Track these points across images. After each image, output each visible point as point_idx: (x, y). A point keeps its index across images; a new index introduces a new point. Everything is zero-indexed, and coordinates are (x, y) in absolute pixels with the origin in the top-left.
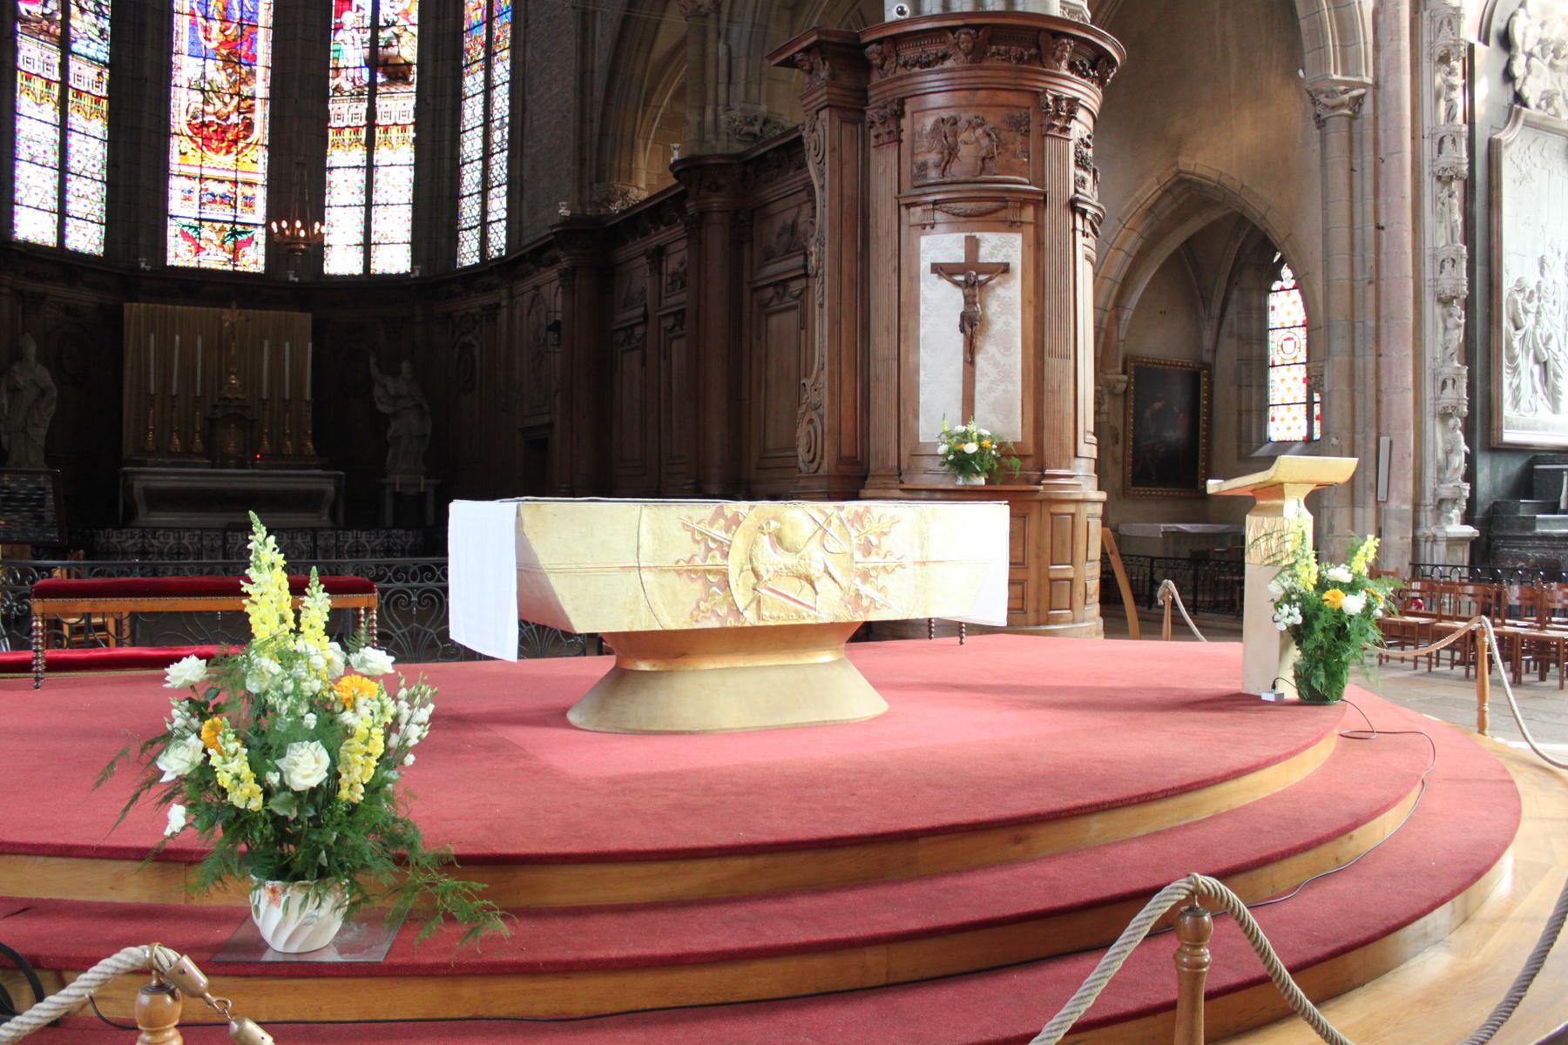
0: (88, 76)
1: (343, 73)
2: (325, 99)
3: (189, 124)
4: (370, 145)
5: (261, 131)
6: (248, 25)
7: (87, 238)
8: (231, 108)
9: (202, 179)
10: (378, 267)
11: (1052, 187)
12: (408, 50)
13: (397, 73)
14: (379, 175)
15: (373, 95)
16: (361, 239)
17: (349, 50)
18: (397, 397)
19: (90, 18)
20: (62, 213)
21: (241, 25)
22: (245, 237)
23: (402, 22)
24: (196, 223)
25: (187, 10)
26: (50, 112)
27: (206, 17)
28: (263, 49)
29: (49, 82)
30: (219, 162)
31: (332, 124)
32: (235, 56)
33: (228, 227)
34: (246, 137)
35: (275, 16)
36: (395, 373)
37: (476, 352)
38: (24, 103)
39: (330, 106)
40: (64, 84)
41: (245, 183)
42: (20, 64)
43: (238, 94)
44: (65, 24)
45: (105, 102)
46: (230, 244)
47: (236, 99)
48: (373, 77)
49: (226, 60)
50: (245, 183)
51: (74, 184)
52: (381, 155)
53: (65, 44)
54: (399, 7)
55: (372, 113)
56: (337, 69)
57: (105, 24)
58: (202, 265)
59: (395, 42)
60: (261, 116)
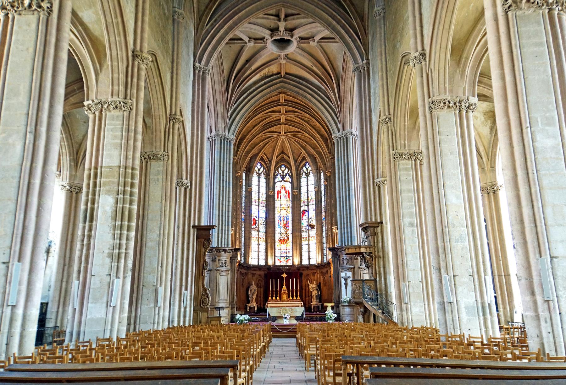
0: (262, 235)
2: (301, 232)
4: (309, 240)
5: (291, 240)
6: (288, 220)
7: (262, 263)
10: (311, 263)
12: (314, 223)
13: (312, 227)
17: (304, 223)
20: (258, 259)
26: (257, 242)
28: (290, 225)
30: (284, 246)
32: (286, 227)
36: (313, 283)
40: (258, 238)
44: (259, 228)
52: (311, 242)
53: (258, 231)
55: (309, 235)
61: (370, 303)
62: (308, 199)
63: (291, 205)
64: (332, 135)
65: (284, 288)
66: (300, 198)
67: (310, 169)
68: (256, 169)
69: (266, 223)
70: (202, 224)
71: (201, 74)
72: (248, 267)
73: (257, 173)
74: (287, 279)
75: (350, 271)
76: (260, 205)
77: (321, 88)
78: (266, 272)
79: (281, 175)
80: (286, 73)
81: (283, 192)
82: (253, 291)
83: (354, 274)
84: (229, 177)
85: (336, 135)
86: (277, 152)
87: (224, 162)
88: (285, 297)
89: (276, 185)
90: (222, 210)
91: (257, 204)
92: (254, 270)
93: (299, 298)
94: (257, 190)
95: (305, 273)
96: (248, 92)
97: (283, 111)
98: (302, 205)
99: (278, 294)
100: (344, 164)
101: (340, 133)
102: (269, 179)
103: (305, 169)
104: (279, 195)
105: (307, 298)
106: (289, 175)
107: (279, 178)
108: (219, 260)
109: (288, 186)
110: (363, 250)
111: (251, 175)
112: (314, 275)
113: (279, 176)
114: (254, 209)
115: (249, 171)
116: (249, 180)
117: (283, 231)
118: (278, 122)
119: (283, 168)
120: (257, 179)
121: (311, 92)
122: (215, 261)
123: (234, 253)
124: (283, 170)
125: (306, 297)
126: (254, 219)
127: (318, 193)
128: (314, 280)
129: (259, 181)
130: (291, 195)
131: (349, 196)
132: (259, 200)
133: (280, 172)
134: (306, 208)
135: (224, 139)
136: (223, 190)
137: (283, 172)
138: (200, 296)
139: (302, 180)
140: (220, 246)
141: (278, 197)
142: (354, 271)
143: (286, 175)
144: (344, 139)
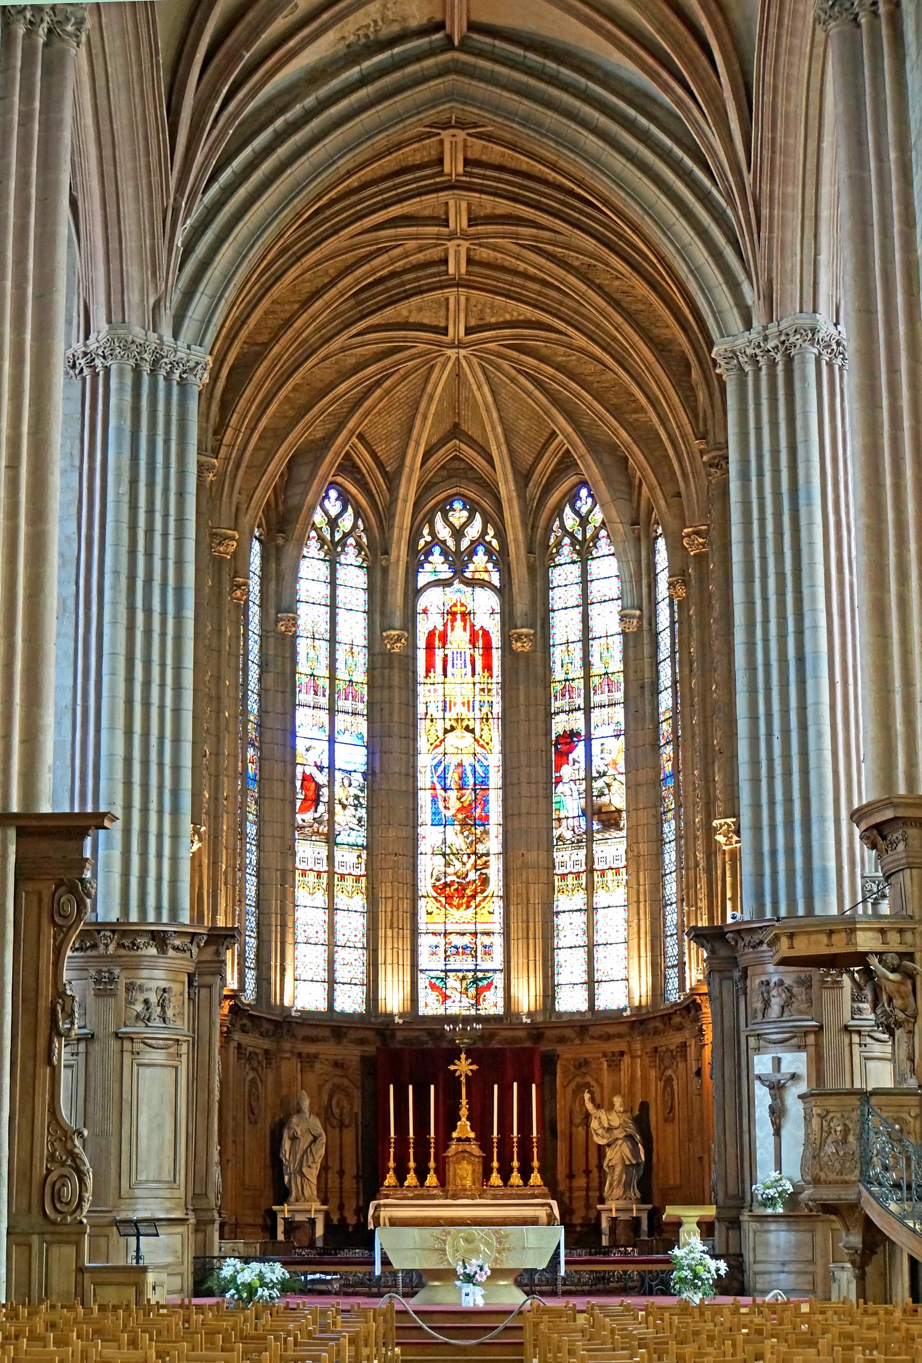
0: (349, 860)
1: (564, 822)
2: (550, 849)
3: (434, 886)
4: (590, 889)
5: (496, 885)
6: (482, 785)
7: (351, 1001)
8: (468, 866)
9: (446, 934)
10: (601, 1004)
11: (828, 1020)
13: (610, 820)
14: (600, 916)
15: (591, 840)
16: (585, 978)
17: (569, 801)
18: (610, 1129)
19: (351, 810)
20: (332, 982)
21: (475, 790)
22: (485, 982)
23: (611, 771)
24: (442, 975)
25: (429, 785)
26: (321, 899)
27: (445, 789)
29: (319, 874)
30: (460, 917)
31: (557, 871)
32: (471, 819)
33: (470, 975)
34: (483, 891)
35: (504, 777)
37: (675, 1083)
38: (302, 895)
39: (555, 854)
40: (331, 873)
41: (483, 933)
42: (297, 865)
43: (475, 853)
45: (363, 879)
46: (472, 991)
47: (473, 857)
48: (589, 824)
49: (463, 824)
50: (483, 933)
51: (341, 955)
53: (331, 840)
54: (609, 759)
56: (559, 820)
57: (362, 812)
58: (449, 1012)
59: (606, 791)
60: (495, 870)
61: (893, 1207)
62: (587, 677)
63: (497, 709)
64: (710, 344)
65: (464, 1129)
66: (548, 669)
67: (597, 517)
68: (319, 518)
69: (370, 798)
70: (46, 808)
71: (41, 41)
72: (277, 1024)
73: (321, 539)
74: (479, 1088)
75: (799, 1048)
76: (341, 704)
77: (654, 100)
78: (371, 1049)
79: (445, 553)
80: (473, 27)
81: (459, 637)
82: (304, 1143)
83: (817, 1062)
84: (180, 562)
85: (732, 340)
86: (424, 433)
87: (151, 484)
88: (465, 1172)
89: (423, 602)
90: (146, 734)
91: (324, 701)
92: (308, 1039)
93: (536, 1178)
94: (323, 628)
95: (566, 1054)
96: (279, 123)
97: (459, 221)
98: (555, 705)
99: (427, 1160)
100: (777, 494)
101: (754, 335)
102: (385, 571)
103: (570, 520)
104: (439, 654)
105: (581, 1182)
106: (489, 552)
107: (437, 566)
108: (130, 987)
109: (485, 607)
110: (866, 941)
111: (290, 549)
112: (615, 1061)
113: (437, 557)
114: (308, 723)
115: (282, 528)
116: (279, 577)
117: (456, 839)
118: (430, 275)
119: (459, 516)
120: (323, 570)
121: (603, 121)
122: (113, 994)
123: (208, 954)
124: (460, 522)
125: (571, 1176)
126: (307, 778)
127: (638, 640)
128: (616, 1091)
129: (333, 583)
130: (496, 655)
131: (801, 659)
132: (332, 678)
133: (444, 533)
134: (577, 722)
135: (155, 363)
136: (148, 632)
137: (458, 534)
138: (41, 1166)
139: (558, 576)
140: (134, 917)
141: (430, 666)
142: (818, 1045)
143: (472, 552)
144: (773, 364)
